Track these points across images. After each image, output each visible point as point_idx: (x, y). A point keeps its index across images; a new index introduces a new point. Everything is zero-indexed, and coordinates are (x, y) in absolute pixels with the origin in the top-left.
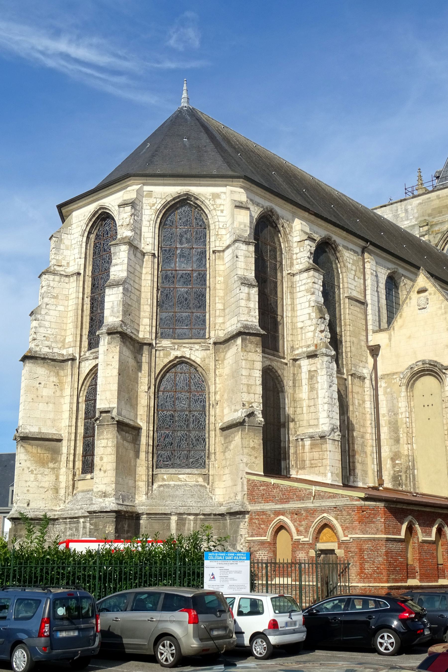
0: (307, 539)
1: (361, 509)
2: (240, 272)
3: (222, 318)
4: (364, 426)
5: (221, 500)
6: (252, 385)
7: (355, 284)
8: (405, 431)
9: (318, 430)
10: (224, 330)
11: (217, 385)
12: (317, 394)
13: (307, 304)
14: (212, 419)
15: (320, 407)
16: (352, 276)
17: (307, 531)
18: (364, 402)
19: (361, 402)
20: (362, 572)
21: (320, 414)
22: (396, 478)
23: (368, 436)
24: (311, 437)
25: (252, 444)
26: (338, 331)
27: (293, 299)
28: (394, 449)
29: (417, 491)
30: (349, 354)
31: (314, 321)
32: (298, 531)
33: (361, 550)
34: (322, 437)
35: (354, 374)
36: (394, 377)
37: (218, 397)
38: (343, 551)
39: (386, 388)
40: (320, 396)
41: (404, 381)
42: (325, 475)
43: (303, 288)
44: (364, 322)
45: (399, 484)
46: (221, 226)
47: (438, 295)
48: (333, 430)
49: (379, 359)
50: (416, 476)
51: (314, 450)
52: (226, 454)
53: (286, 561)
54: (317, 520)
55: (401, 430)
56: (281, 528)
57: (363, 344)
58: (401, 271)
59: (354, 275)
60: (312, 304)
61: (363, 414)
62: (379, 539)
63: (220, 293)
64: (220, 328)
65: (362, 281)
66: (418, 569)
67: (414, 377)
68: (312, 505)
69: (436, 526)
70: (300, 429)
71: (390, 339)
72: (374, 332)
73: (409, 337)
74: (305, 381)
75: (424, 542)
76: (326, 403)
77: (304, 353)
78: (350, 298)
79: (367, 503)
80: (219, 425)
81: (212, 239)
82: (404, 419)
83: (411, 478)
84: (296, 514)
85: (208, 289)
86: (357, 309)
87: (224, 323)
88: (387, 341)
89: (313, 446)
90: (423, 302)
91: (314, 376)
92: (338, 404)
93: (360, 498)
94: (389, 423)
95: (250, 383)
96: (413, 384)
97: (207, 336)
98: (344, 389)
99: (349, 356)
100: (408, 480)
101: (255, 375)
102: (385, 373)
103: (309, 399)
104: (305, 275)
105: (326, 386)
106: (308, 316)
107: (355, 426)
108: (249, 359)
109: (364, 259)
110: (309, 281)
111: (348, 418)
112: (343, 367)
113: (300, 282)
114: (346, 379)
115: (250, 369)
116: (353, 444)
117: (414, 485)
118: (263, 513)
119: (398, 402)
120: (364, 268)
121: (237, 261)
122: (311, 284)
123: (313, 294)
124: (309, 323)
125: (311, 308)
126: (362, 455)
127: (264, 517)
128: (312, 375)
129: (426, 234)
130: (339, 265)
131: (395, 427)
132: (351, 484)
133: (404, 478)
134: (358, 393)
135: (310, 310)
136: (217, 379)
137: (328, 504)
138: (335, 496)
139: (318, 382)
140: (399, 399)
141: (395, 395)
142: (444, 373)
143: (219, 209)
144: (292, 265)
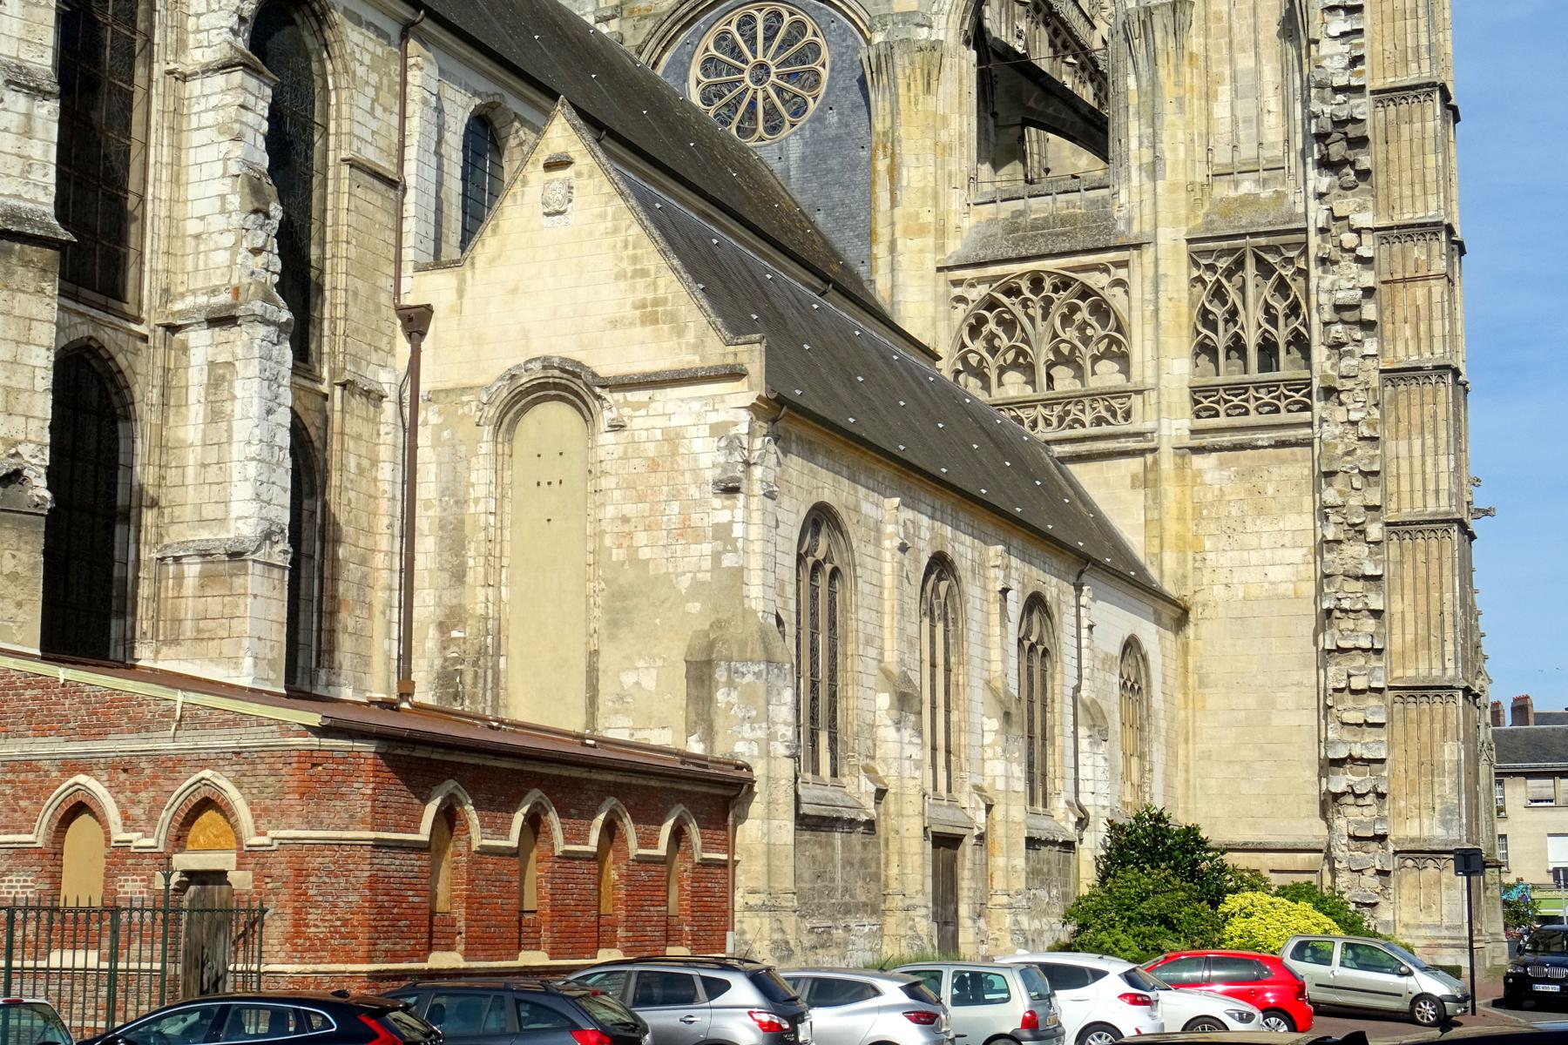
0: (151, 842)
1: (310, 759)
4: (370, 532)
6: (20, 391)
7: (374, 125)
9: (223, 536)
12: (229, 430)
13: (218, 168)
15: (235, 469)
16: (366, 104)
17: (152, 819)
18: (375, 463)
19: (365, 463)
20: (298, 934)
21: (233, 490)
22: (447, 679)
23: (379, 560)
24: (204, 554)
26: (313, 257)
27: (177, 148)
28: (449, 598)
29: (502, 715)
30: (341, 325)
31: (236, 220)
32: (126, 817)
33: (301, 873)
34: (235, 555)
35: (352, 383)
36: (465, 399)
38: (250, 875)
39: (439, 428)
40: (236, 437)
41: (491, 412)
42: (235, 661)
43: (209, 118)
44: (391, 237)
45: (456, 696)
47: (600, 178)
48: (268, 535)
49: (426, 345)
50: (502, 675)
51: (208, 592)
53: (84, 903)
54: (182, 790)
55: (472, 546)
56: (78, 808)
57: (385, 299)
58: (513, 104)
59: (373, 101)
60: (234, 168)
61: (370, 496)
62: (354, 843)
65: (395, 120)
66: (461, 925)
67: (517, 402)
68: (171, 746)
69: (525, 809)
70: (174, 529)
71: (461, 293)
72: (420, 268)
73: (514, 291)
74: (196, 393)
75: (486, 851)
76: (253, 459)
78: (354, 164)
79: (328, 742)
82: (483, 517)
83: (490, 680)
84: (125, 770)
86: (374, 198)
88: (454, 296)
89: (206, 579)
90: (557, 193)
91: (223, 378)
92: (288, 463)
93: (309, 728)
94: (441, 528)
95: (13, 384)
96: (515, 421)
98: (318, 422)
99: (340, 331)
100: (481, 685)
102: (440, 386)
103: (204, 445)
104: (219, 80)
105: (256, 409)
106: (217, 202)
107: (344, 528)
108: (17, 312)
109: (405, 57)
110: (229, 99)
111: (325, 505)
112: (320, 361)
113: (203, 101)
114: (325, 397)
115: (17, 342)
116: (335, 579)
117: (496, 697)
118: (29, 764)
119: (469, 469)
120: (404, 83)
122: (233, 110)
123: (238, 138)
124: (219, 222)
125: (229, 181)
126: (358, 612)
127: (31, 776)
128: (218, 377)
129: (614, 17)
130: (329, 67)
131: (454, 538)
132: (320, 690)
133: (468, 679)
134: (359, 437)
135: (224, 186)
137: (217, 744)
138: (238, 720)
139: (234, 398)
140: (473, 460)
141: (463, 450)
142: (599, 397)
144: (181, 47)
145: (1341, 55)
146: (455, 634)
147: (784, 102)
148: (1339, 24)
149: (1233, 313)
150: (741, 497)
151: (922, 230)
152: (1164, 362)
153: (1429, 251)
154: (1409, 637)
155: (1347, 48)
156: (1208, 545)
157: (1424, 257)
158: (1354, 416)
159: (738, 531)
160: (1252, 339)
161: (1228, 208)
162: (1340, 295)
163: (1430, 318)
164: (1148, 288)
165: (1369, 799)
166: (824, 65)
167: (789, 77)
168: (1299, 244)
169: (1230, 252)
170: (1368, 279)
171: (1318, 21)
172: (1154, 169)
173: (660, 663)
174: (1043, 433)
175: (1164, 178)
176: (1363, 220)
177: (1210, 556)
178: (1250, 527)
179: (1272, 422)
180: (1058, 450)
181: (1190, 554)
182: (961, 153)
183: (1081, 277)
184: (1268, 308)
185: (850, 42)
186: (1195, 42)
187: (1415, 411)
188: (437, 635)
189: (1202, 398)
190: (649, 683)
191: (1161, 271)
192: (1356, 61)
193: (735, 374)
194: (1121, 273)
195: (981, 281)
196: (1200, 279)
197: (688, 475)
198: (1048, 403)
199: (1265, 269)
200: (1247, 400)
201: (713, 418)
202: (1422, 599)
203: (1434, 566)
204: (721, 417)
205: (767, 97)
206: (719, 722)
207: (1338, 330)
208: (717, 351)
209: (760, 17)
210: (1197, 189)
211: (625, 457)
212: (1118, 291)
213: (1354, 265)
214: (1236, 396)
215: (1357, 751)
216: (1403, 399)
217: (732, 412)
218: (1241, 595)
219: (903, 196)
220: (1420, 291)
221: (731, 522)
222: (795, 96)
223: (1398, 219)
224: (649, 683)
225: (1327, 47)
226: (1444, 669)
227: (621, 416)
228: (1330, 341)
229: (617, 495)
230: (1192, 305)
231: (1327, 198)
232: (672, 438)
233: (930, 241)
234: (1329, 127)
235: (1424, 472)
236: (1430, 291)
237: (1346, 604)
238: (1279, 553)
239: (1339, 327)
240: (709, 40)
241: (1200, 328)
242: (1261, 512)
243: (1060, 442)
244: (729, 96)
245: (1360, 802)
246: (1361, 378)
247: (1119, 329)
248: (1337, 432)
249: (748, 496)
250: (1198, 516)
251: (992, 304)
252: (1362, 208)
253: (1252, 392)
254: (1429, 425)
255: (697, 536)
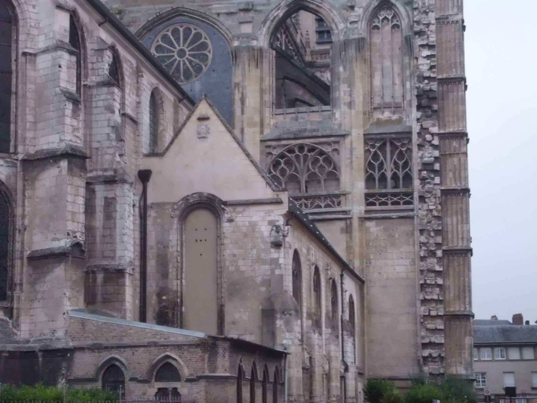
2: (63, 84)
3: (32, 132)
5: (27, 336)
8: (176, 265)
9: (113, 263)
10: (35, 146)
11: (26, 208)
13: (106, 123)
14: (18, 246)
25: (74, 277)
37: (26, 222)
39: (155, 218)
41: (177, 213)
43: (101, 104)
46: (33, 24)
52: (38, 287)
55: (171, 264)
63: (31, 103)
64: (30, 144)
77: (99, 177)
80: (27, 253)
81: (22, 37)
83: (179, 315)
85: (13, 97)
87: (34, 138)
89: (106, 281)
95: (74, 211)
97: (12, 150)
101: (79, 202)
102: (155, 201)
103: (104, 228)
106: (106, 137)
108: (74, 184)
113: (97, 96)
115: (75, 195)
119: (169, 234)
121: (60, 71)
124: (107, 143)
125: (110, 128)
136: (26, 201)
140: (171, 231)
143: (31, 3)
145: (427, 64)
146: (164, 298)
147: (192, 67)
148: (426, 52)
149: (381, 165)
150: (282, 248)
151: (253, 125)
152: (353, 182)
153: (460, 143)
154: (452, 295)
155: (429, 62)
156: (372, 257)
157: (457, 146)
158: (431, 207)
159: (281, 261)
160: (389, 175)
161: (379, 123)
162: (426, 159)
163: (460, 170)
164: (348, 153)
165: (437, 360)
166: (209, 52)
167: (194, 56)
168: (407, 138)
169: (381, 139)
170: (437, 153)
171: (418, 50)
172: (350, 105)
173: (249, 310)
174: (305, 211)
175: (355, 109)
176: (435, 130)
177: (373, 261)
178: (389, 250)
179: (398, 209)
180: (311, 217)
181: (365, 261)
182: (270, 93)
183: (319, 147)
184: (396, 164)
185: (222, 43)
186: (367, 54)
187: (454, 206)
188: (156, 298)
189: (370, 199)
190: (245, 317)
191: (354, 146)
192: (432, 67)
193: (279, 202)
194: (336, 146)
195: (278, 146)
196: (368, 150)
197: (259, 240)
198: (307, 198)
199: (394, 147)
200: (387, 199)
201: (269, 218)
202: (457, 281)
203: (462, 268)
204: (271, 218)
205: (184, 64)
206: (278, 333)
207: (424, 173)
208: (267, 193)
209: (181, 30)
210: (367, 114)
211: (234, 232)
212: (335, 154)
213: (431, 148)
214: (383, 197)
215: (433, 340)
216: (449, 202)
217: (276, 216)
218: (385, 277)
219: (247, 110)
220: (455, 160)
221: (278, 258)
222: (197, 64)
223: (447, 131)
224: (245, 317)
225: (421, 61)
226: (466, 308)
227: (231, 216)
228: (421, 177)
229: (231, 246)
230: (366, 160)
231: (420, 121)
232: (253, 226)
233: (258, 129)
234: (422, 93)
235: (457, 230)
236: (460, 159)
237: (428, 282)
238: (401, 262)
239: (425, 172)
240: (159, 38)
241: (368, 170)
242: (393, 244)
243: (312, 214)
244: (168, 62)
245: (434, 360)
246: (434, 193)
247: (335, 168)
248: (425, 213)
249: (285, 248)
250: (368, 245)
251: (282, 156)
252: (434, 125)
253: (389, 196)
254: (459, 212)
255: (264, 262)
